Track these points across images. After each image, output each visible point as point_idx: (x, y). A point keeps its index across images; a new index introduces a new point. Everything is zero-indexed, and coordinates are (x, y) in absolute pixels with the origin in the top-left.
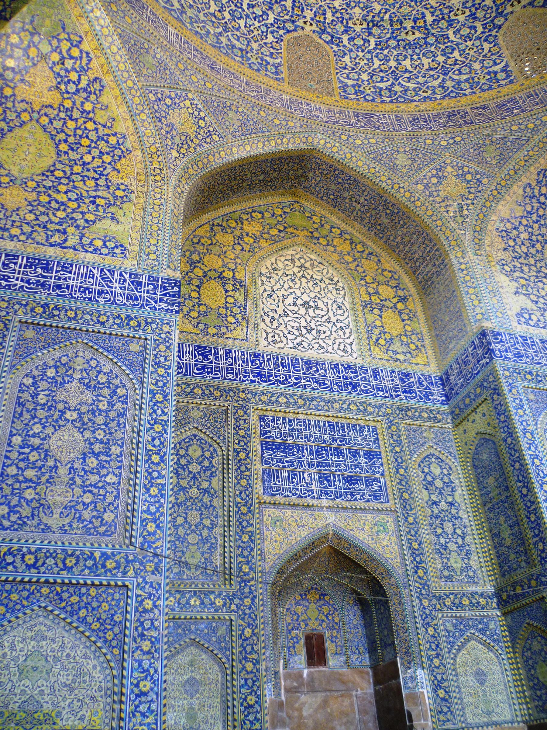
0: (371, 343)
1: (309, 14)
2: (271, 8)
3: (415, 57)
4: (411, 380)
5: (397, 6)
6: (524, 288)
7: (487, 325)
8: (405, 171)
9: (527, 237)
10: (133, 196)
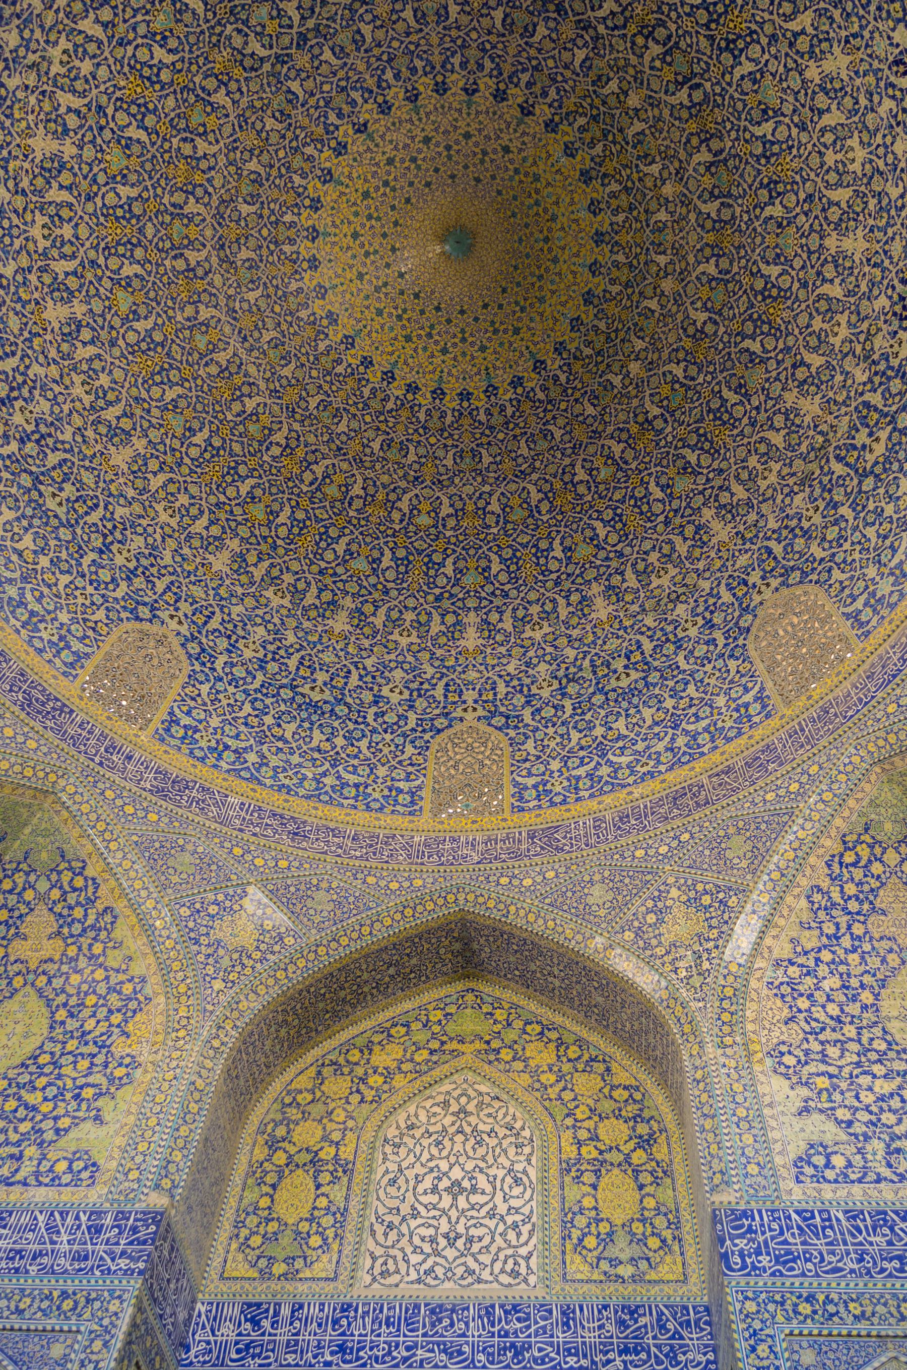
0: (569, 1247)
1: (470, 696)
2: (411, 707)
3: (632, 711)
4: (642, 1321)
5: (600, 642)
6: (825, 1095)
7: (726, 1198)
8: (602, 913)
9: (839, 984)
10: (138, 1073)
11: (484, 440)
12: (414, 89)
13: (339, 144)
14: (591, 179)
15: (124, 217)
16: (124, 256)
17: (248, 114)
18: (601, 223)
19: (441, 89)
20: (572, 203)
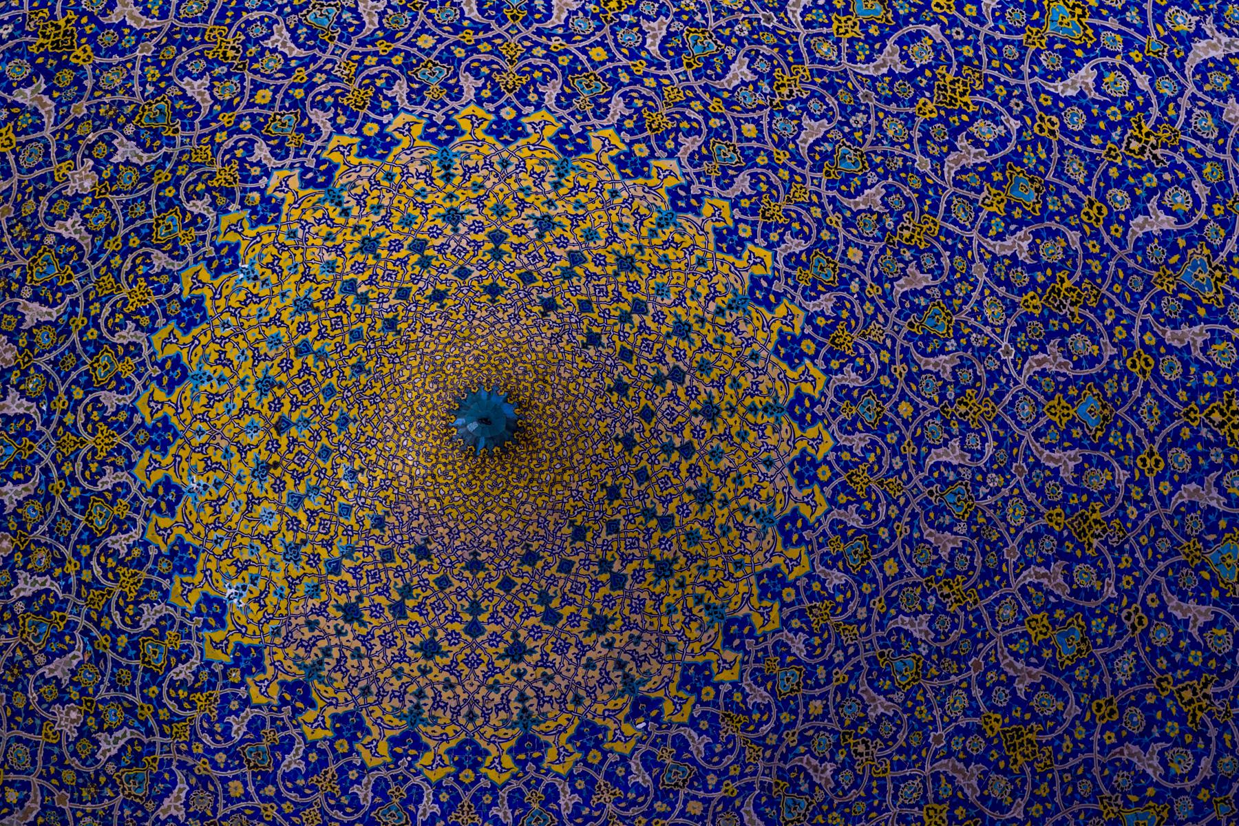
11: (469, 37)
12: (522, 764)
13: (696, 690)
14: (173, 554)
15: (1168, 715)
16: (1194, 645)
17: (861, 807)
18: (154, 465)
19: (468, 754)
20: (217, 504)
